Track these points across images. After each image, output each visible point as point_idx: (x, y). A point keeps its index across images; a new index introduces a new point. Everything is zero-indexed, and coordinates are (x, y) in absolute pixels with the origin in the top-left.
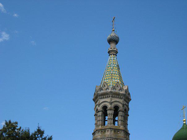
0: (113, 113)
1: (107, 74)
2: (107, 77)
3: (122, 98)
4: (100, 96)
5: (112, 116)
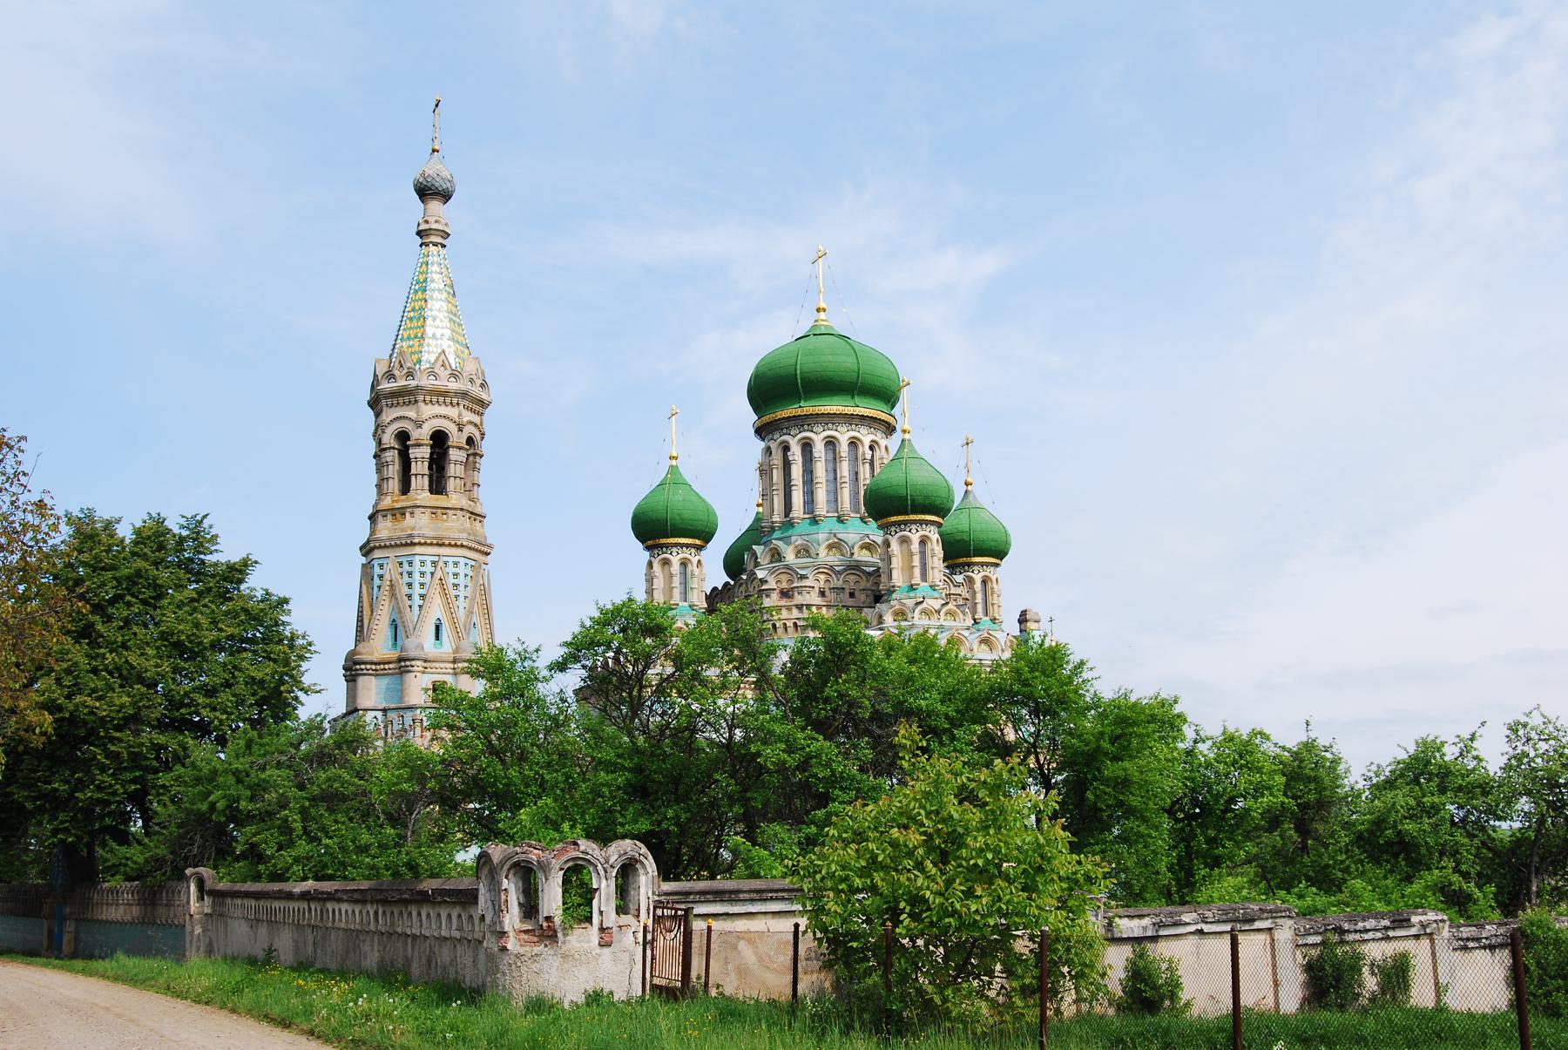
0: (428, 456)
1: (411, 319)
2: (411, 328)
3: (458, 404)
4: (386, 398)
5: (426, 464)
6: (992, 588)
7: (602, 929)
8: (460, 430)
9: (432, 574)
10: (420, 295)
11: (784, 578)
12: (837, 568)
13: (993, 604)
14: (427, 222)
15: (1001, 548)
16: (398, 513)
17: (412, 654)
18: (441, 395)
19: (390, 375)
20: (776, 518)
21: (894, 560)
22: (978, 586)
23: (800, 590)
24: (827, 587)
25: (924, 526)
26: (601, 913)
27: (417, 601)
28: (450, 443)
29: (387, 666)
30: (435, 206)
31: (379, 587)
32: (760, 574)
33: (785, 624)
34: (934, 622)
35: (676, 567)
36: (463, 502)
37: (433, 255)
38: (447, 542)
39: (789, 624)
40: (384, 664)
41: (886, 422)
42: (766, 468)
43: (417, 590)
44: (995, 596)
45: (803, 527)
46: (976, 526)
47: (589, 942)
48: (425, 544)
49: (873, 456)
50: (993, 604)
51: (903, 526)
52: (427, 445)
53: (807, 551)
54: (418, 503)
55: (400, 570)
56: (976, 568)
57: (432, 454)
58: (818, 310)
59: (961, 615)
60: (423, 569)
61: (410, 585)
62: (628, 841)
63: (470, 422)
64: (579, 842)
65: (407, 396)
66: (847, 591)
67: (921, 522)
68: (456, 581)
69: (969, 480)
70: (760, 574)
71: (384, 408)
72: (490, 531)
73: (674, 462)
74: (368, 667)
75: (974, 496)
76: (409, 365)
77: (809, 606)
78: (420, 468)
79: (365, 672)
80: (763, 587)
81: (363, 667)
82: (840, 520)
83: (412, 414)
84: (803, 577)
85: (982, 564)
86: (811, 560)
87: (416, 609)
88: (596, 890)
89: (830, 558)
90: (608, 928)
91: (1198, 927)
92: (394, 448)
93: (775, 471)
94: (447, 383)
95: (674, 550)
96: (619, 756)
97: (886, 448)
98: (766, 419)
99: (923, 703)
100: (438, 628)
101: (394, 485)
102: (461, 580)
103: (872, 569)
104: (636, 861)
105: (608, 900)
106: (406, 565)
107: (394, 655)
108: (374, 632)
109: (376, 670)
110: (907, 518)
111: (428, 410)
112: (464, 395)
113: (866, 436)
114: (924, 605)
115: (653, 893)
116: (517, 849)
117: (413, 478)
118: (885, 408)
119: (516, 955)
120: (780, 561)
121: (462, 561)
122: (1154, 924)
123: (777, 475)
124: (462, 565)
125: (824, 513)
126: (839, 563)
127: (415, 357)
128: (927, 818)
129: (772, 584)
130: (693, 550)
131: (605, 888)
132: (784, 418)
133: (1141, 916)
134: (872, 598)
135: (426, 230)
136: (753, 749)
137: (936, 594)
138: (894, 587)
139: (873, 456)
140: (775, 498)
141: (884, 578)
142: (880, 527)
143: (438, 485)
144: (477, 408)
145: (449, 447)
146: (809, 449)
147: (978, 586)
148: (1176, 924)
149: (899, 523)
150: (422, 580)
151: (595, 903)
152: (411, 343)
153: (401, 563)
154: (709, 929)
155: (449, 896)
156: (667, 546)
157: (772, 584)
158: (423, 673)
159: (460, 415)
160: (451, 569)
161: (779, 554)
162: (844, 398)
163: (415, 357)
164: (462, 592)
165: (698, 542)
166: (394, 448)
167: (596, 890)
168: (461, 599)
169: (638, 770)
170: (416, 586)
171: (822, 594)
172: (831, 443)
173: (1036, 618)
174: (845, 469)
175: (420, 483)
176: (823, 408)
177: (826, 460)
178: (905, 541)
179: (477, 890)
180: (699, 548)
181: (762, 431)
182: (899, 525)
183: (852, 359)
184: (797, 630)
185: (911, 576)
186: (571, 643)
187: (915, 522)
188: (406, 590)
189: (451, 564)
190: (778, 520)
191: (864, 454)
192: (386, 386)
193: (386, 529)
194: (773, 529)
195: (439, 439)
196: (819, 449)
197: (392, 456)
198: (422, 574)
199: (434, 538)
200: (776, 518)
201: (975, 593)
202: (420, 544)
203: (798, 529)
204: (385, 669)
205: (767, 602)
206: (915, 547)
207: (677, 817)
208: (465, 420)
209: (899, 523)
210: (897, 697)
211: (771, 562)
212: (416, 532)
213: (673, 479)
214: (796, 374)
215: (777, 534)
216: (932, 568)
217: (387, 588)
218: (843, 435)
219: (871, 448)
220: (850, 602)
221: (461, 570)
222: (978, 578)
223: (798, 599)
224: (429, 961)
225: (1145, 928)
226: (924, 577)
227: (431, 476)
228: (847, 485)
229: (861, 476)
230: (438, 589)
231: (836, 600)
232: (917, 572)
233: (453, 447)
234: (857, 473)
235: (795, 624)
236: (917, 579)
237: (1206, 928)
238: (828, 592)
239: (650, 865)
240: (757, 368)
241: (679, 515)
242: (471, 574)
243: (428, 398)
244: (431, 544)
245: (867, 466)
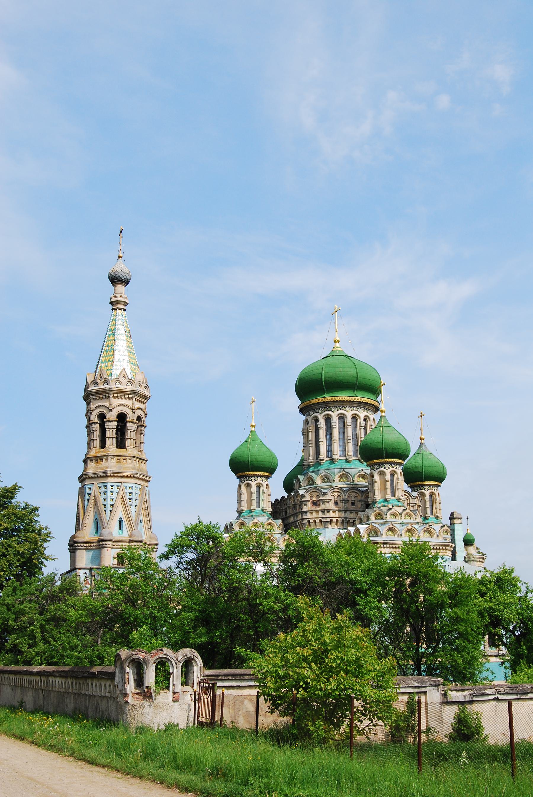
0: (116, 427)
1: (106, 351)
3: (132, 398)
4: (92, 395)
5: (115, 432)
6: (436, 499)
7: (174, 693)
8: (133, 412)
9: (117, 493)
10: (111, 338)
11: (314, 494)
12: (344, 489)
13: (436, 508)
14: (115, 297)
15: (441, 476)
16: (99, 459)
17: (106, 537)
18: (123, 393)
19: (95, 383)
20: (311, 460)
21: (376, 484)
22: (427, 498)
23: (323, 501)
24: (339, 499)
25: (393, 465)
26: (174, 685)
27: (109, 508)
28: (127, 420)
29: (92, 545)
30: (120, 288)
31: (88, 500)
32: (301, 492)
33: (315, 521)
34: (398, 520)
35: (254, 488)
36: (135, 453)
37: (119, 315)
38: (126, 475)
39: (317, 520)
40: (91, 543)
41: (373, 405)
42: (305, 431)
43: (109, 502)
44: (438, 503)
45: (326, 465)
46: (426, 464)
47: (168, 699)
48: (114, 476)
49: (366, 424)
50: (436, 508)
51: (381, 465)
52: (115, 421)
53: (328, 479)
54: (110, 453)
55: (100, 491)
56: (426, 487)
57: (117, 426)
58: (335, 342)
59: (414, 516)
60: (112, 490)
61: (105, 499)
62: (188, 649)
63: (139, 408)
64: (163, 649)
65: (104, 394)
66: (350, 502)
67: (391, 463)
68: (131, 497)
69: (423, 437)
70: (301, 492)
71: (92, 401)
72: (149, 468)
73: (253, 429)
74: (82, 545)
75: (426, 447)
76: (105, 377)
77: (328, 511)
78: (111, 434)
79: (80, 547)
80: (303, 500)
81: (79, 544)
82: (347, 461)
83: (107, 404)
84: (325, 494)
85: (430, 485)
86: (330, 484)
87: (108, 512)
88: (172, 673)
89: (341, 483)
90: (177, 692)
91: (496, 696)
92: (97, 423)
93: (310, 433)
94: (126, 387)
95: (253, 478)
96: (194, 604)
97: (374, 419)
98: (305, 404)
99: (353, 576)
100: (120, 523)
101: (97, 443)
102: (134, 496)
103: (365, 489)
104: (192, 659)
105: (177, 678)
106: (103, 488)
107: (96, 538)
108: (85, 525)
109: (86, 546)
110: (383, 461)
111: (115, 402)
112: (135, 393)
113: (362, 413)
114: (393, 510)
115: (201, 675)
116: (134, 653)
117: (107, 439)
118: (373, 397)
119: (132, 705)
120: (313, 484)
121: (134, 486)
122: (470, 695)
123: (311, 436)
124: (134, 488)
125: (338, 457)
126: (346, 486)
127: (109, 372)
128: (315, 642)
129: (308, 498)
130: (264, 479)
131: (176, 672)
132: (315, 403)
133: (463, 690)
134: (365, 505)
135: (115, 301)
136: (258, 601)
137: (400, 504)
138: (376, 500)
139: (366, 424)
140: (311, 448)
141: (370, 495)
142: (368, 466)
143: (121, 444)
144: (143, 400)
145: (127, 422)
146: (329, 421)
147: (427, 498)
148: (482, 695)
149: (379, 464)
150: (112, 496)
151: (171, 679)
152: (107, 364)
153: (100, 487)
154: (223, 693)
155: (105, 675)
156: (249, 476)
157: (308, 498)
158: (112, 548)
159: (133, 404)
160: (128, 490)
161: (312, 481)
162: (349, 392)
163: (109, 372)
164: (134, 503)
165: (266, 474)
166: (97, 423)
167: (172, 673)
168: (134, 506)
169: (202, 611)
170: (109, 500)
171: (336, 503)
172: (342, 418)
173: (460, 517)
174: (350, 432)
175: (111, 442)
176: (337, 398)
177: (339, 427)
178: (382, 474)
179: (115, 672)
180: (267, 477)
181: (303, 410)
182: (379, 465)
183: (354, 370)
184: (322, 524)
185: (386, 494)
186: (171, 545)
187: (387, 463)
188: (103, 502)
189: (128, 487)
190: (312, 461)
191: (360, 423)
192: (92, 388)
193: (92, 468)
194: (309, 466)
195: (122, 418)
196: (335, 421)
197: (96, 427)
198: (112, 493)
199: (118, 473)
200: (311, 460)
201: (425, 502)
202: (111, 476)
203: (323, 466)
204: (91, 546)
205: (305, 508)
206: (388, 477)
207: (221, 635)
208: (136, 407)
209: (379, 464)
210: (338, 573)
211: (308, 485)
212: (108, 470)
213: (253, 438)
214: (322, 378)
215: (312, 469)
216: (398, 489)
217: (93, 501)
218: (349, 413)
219: (365, 420)
220: (352, 508)
221: (134, 490)
222: (427, 493)
223: (322, 506)
224: (96, 708)
225: (465, 697)
226: (393, 494)
227: (117, 438)
228: (351, 441)
229: (359, 436)
230: (121, 501)
231: (344, 507)
232: (389, 491)
233: (129, 422)
234: (356, 434)
235: (321, 521)
236: (389, 495)
237: (500, 697)
238: (339, 503)
239: (199, 661)
240: (300, 375)
241: (256, 459)
242: (139, 492)
243: (115, 395)
244: (117, 476)
245: (363, 430)
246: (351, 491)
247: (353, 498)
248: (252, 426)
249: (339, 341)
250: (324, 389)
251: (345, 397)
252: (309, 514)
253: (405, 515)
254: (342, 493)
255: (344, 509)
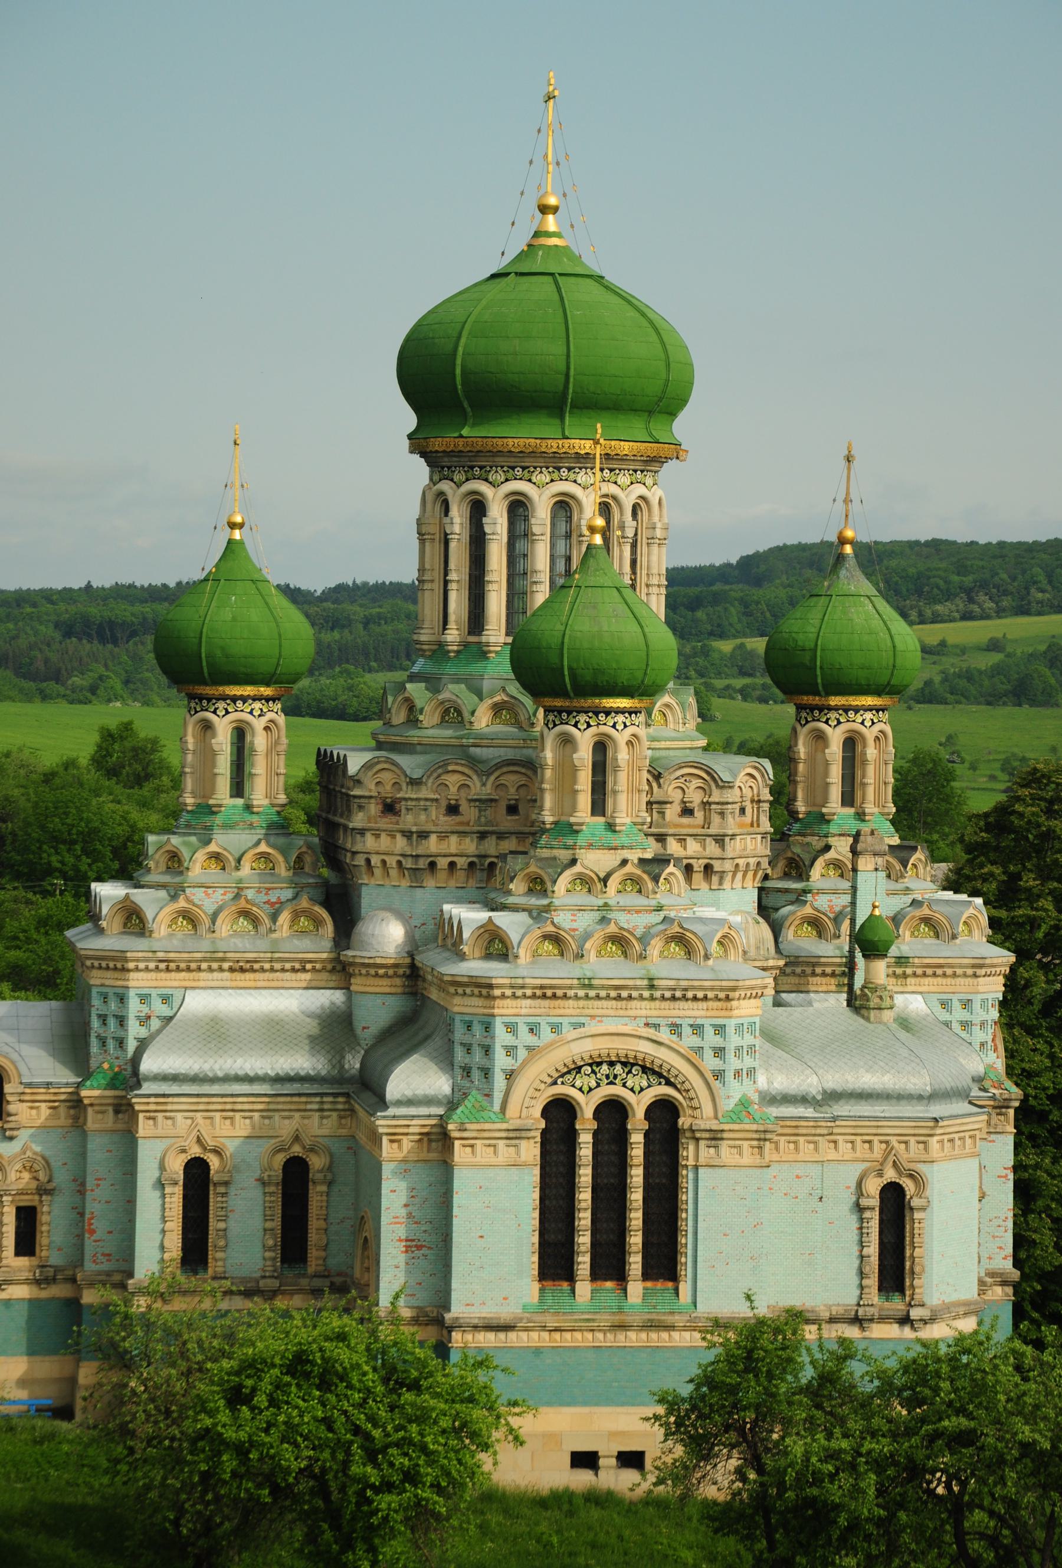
33: (384, 862)
39: (392, 861)
51: (564, 716)
56: (833, 715)
66: (503, 805)
73: (237, 535)
95: (221, 705)
183: (559, 349)
223: (408, 821)
235: (399, 863)
238: (464, 807)
241: (223, 649)
246: (505, 769)
247: (512, 790)
248: (232, 526)
249: (555, 210)
250: (464, 409)
251: (527, 441)
252: (369, 838)
253: (623, 882)
254: (475, 777)
255: (476, 829)
